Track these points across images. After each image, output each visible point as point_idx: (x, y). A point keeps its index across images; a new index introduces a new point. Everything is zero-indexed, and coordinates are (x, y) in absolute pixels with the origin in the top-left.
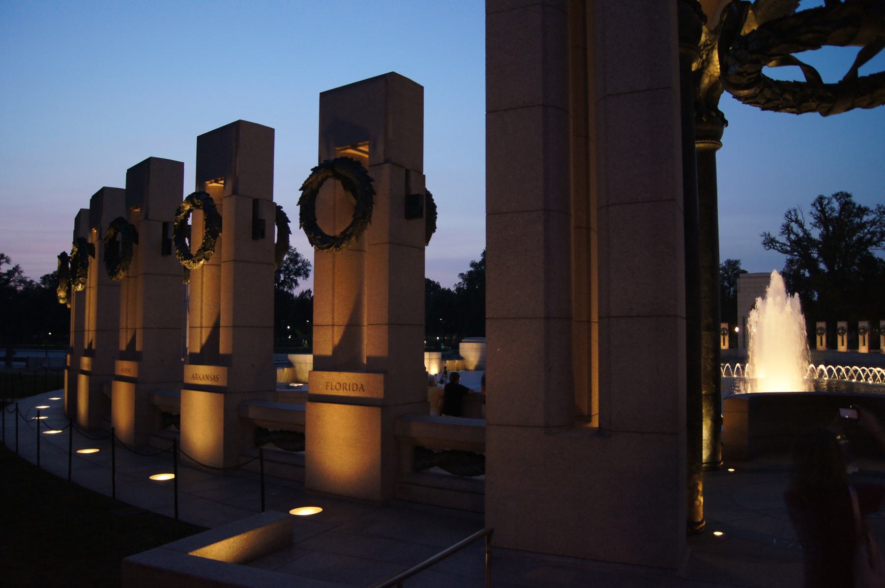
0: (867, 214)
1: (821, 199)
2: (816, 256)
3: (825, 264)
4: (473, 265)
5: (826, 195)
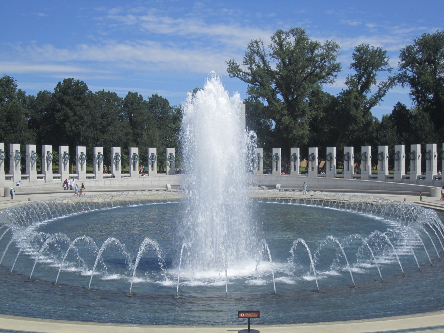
0: (318, 49)
5: (284, 30)
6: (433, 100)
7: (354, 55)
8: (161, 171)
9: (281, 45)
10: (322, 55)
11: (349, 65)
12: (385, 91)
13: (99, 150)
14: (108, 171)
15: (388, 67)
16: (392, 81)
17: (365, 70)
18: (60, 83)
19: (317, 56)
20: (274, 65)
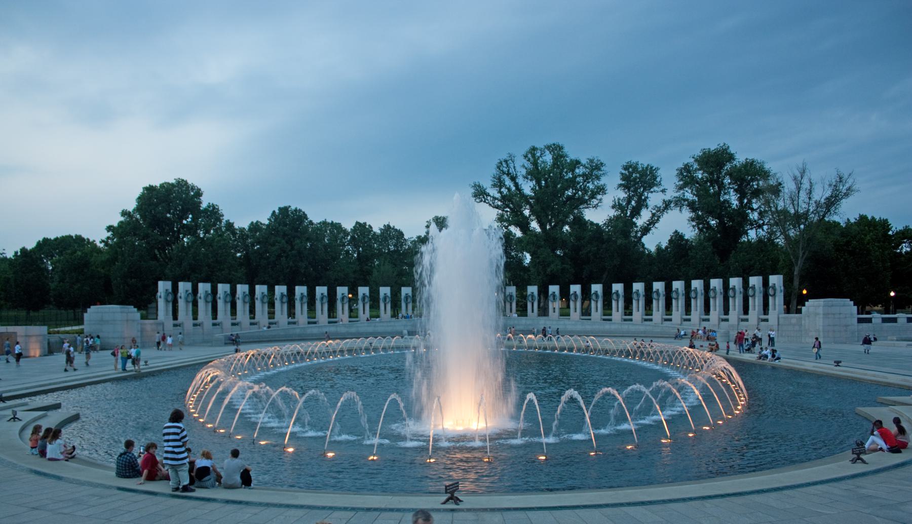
1: (534, 149)
2: (527, 212)
4: (124, 213)
5: (537, 146)
7: (622, 174)
9: (535, 164)
10: (584, 175)
11: (616, 186)
15: (662, 188)
16: (667, 205)
17: (635, 191)
19: (579, 176)
20: (528, 188)
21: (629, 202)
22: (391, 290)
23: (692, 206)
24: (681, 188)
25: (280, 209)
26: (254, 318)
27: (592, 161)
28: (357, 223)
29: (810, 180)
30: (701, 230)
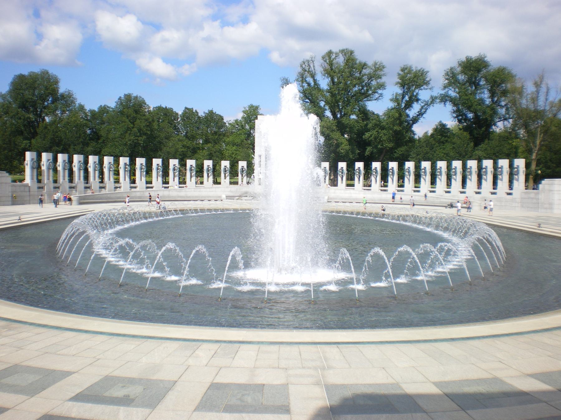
1: (330, 53)
2: (322, 104)
3: (331, 112)
6: (473, 118)
7: (399, 74)
8: (216, 182)
9: (331, 64)
12: (426, 109)
13: (225, 164)
14: (183, 182)
16: (433, 100)
17: (409, 88)
18: (120, 97)
19: (365, 75)
20: (324, 83)
21: (403, 98)
22: (196, 162)
23: (453, 101)
24: (445, 87)
25: (125, 95)
26: (87, 183)
27: (376, 64)
28: (186, 108)
29: (547, 84)
30: (460, 121)
